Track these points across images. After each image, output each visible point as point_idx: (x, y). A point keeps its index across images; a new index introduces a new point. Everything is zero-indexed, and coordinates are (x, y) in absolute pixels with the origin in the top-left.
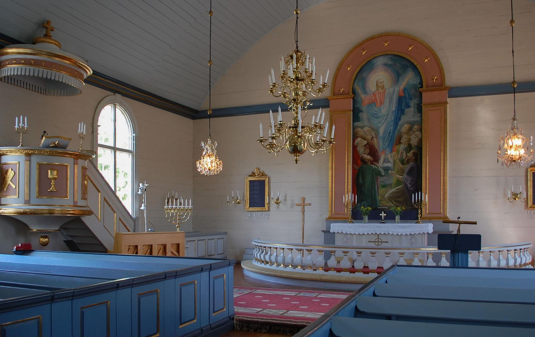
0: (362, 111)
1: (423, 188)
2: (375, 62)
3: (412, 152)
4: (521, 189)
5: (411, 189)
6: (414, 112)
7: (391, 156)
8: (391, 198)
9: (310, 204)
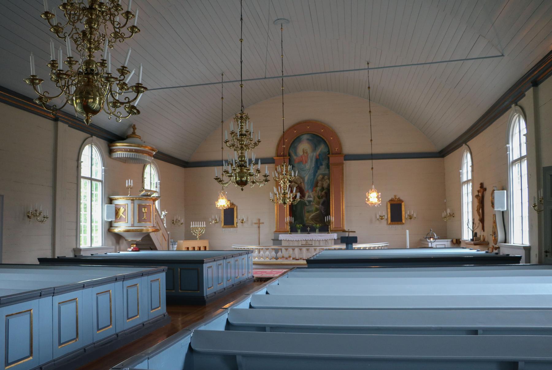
1: (331, 213)
4: (384, 213)
8: (312, 219)
9: (263, 223)
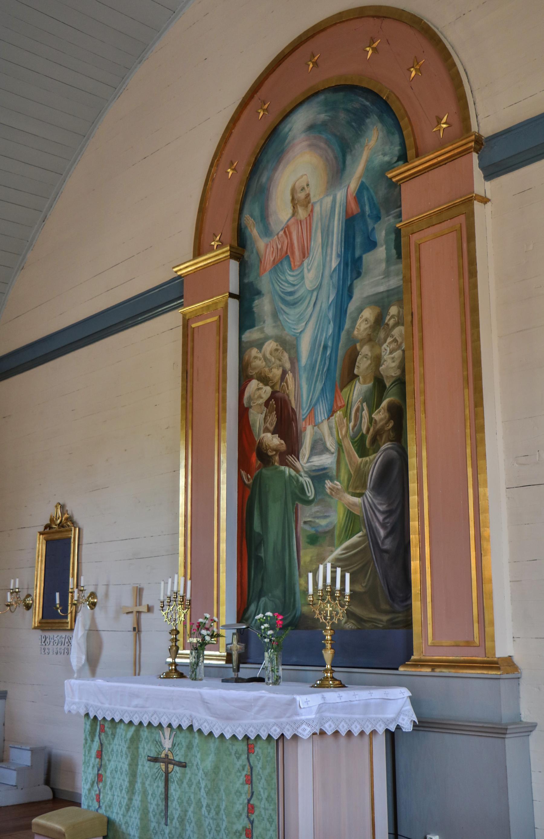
0: (259, 293)
2: (286, 129)
3: (385, 403)
5: (388, 545)
6: (388, 260)
7: (330, 428)
